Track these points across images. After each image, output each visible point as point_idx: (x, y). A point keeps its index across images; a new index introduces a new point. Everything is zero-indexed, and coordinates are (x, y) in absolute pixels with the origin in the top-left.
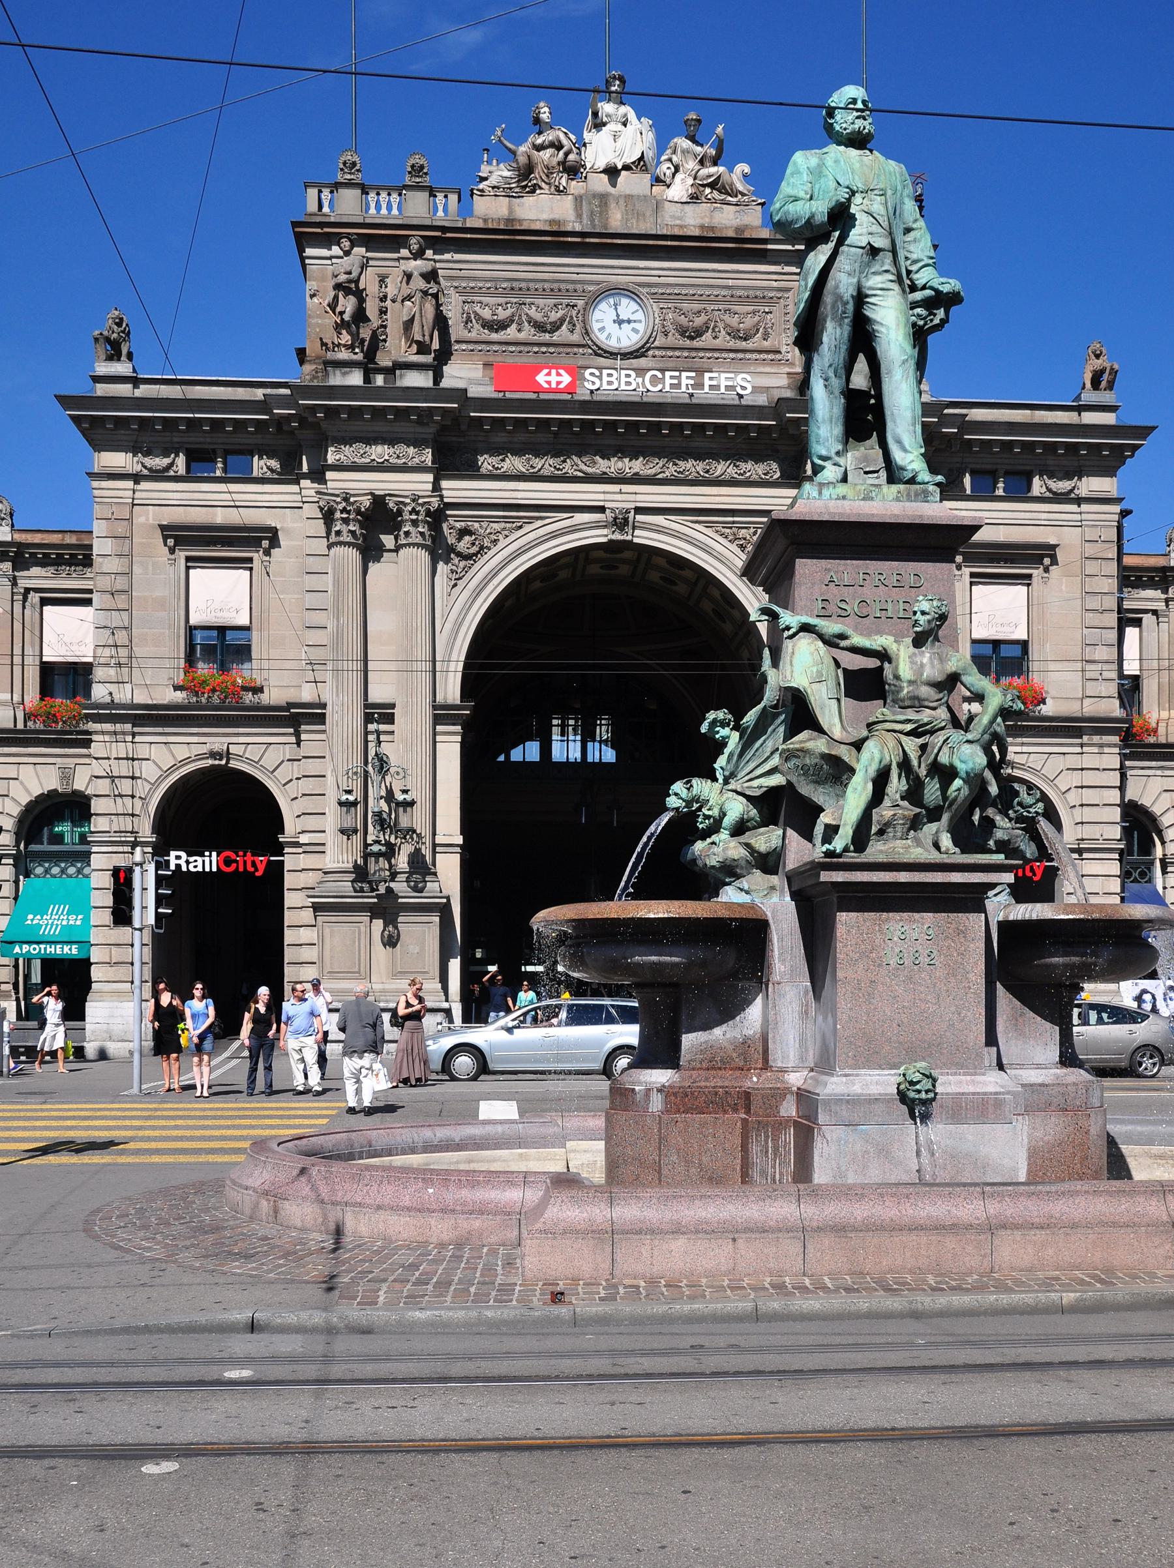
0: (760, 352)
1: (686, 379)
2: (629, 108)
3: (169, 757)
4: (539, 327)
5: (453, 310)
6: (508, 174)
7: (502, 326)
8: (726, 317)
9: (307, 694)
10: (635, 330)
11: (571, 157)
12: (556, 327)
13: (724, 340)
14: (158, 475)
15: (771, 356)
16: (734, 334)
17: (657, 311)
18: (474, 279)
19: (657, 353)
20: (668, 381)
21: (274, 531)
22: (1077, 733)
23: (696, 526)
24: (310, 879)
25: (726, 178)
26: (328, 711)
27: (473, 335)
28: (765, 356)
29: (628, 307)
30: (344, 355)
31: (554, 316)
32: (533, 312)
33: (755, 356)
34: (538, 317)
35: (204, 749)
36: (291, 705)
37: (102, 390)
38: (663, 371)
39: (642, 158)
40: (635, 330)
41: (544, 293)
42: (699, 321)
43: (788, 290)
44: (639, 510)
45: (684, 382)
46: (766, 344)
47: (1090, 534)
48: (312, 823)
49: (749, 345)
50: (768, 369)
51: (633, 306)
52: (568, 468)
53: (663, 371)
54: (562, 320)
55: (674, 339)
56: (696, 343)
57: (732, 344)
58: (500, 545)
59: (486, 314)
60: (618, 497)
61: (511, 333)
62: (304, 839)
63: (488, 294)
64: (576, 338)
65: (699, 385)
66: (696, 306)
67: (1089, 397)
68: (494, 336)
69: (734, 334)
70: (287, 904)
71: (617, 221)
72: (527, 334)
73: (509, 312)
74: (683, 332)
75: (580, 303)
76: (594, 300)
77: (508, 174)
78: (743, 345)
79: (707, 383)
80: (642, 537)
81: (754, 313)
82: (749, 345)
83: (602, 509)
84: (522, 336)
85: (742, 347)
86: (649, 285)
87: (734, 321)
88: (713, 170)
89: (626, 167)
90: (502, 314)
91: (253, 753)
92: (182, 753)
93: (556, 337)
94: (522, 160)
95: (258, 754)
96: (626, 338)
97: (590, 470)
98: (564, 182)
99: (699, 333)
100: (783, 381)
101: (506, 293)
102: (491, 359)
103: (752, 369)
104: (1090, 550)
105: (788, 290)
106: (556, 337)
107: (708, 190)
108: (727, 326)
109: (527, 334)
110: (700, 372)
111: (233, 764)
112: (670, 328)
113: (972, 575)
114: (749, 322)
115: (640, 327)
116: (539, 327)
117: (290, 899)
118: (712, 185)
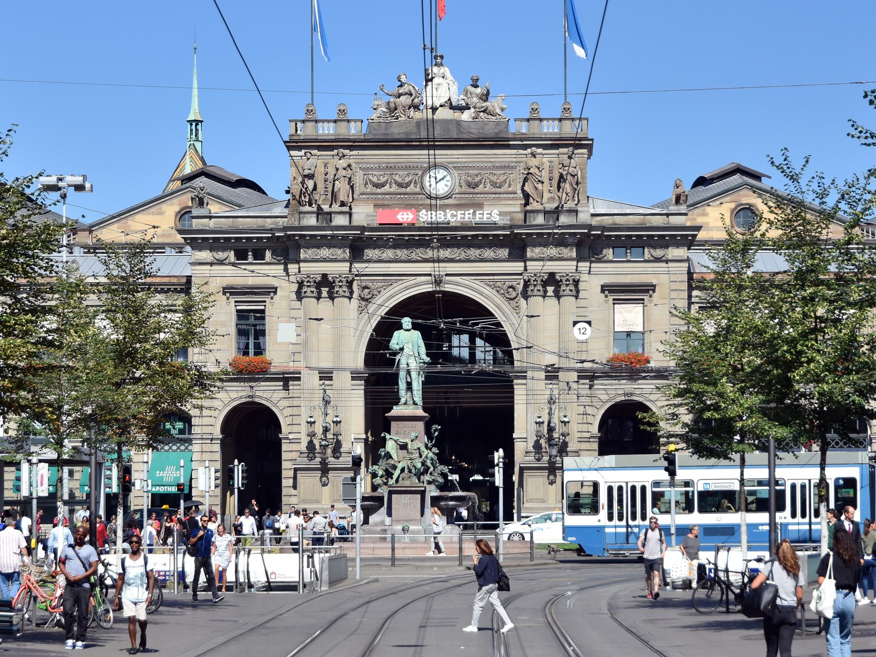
0: (507, 193)
2: (446, 68)
4: (400, 185)
5: (358, 180)
6: (385, 110)
7: (383, 185)
9: (292, 366)
10: (446, 185)
11: (416, 100)
12: (408, 185)
14: (221, 262)
15: (512, 196)
17: (456, 175)
18: (370, 163)
19: (457, 196)
21: (276, 288)
23: (476, 282)
24: (295, 455)
25: (490, 108)
26: (302, 376)
27: (369, 190)
28: (509, 196)
29: (441, 173)
31: (407, 180)
32: (397, 178)
33: (505, 196)
34: (400, 180)
36: (284, 373)
39: (449, 99)
40: (446, 185)
41: (402, 169)
42: (477, 179)
43: (520, 162)
44: (447, 275)
46: (510, 189)
47: (673, 278)
48: (295, 428)
49: (502, 190)
50: (511, 202)
52: (414, 256)
54: (411, 182)
55: (465, 189)
56: (476, 190)
57: (493, 190)
58: (382, 293)
59: (375, 179)
61: (387, 188)
62: (291, 436)
63: (376, 169)
64: (418, 190)
67: (673, 209)
68: (379, 191)
69: (494, 184)
70: (283, 467)
71: (438, 133)
72: (394, 189)
73: (386, 178)
74: (469, 185)
75: (420, 173)
77: (385, 110)
81: (504, 174)
82: (502, 190)
84: (392, 190)
86: (453, 163)
87: (494, 179)
88: (484, 104)
89: (441, 106)
90: (383, 180)
91: (266, 395)
92: (234, 395)
93: (408, 190)
94: (392, 105)
95: (268, 394)
96: (442, 188)
97: (424, 257)
98: (412, 113)
99: (477, 185)
101: (384, 169)
102: (378, 202)
103: (503, 202)
104: (674, 286)
105: (520, 162)
106: (408, 190)
107: (482, 114)
108: (491, 181)
109: (394, 189)
111: (257, 400)
112: (463, 184)
115: (449, 184)
116: (400, 185)
117: (285, 465)
118: (484, 111)
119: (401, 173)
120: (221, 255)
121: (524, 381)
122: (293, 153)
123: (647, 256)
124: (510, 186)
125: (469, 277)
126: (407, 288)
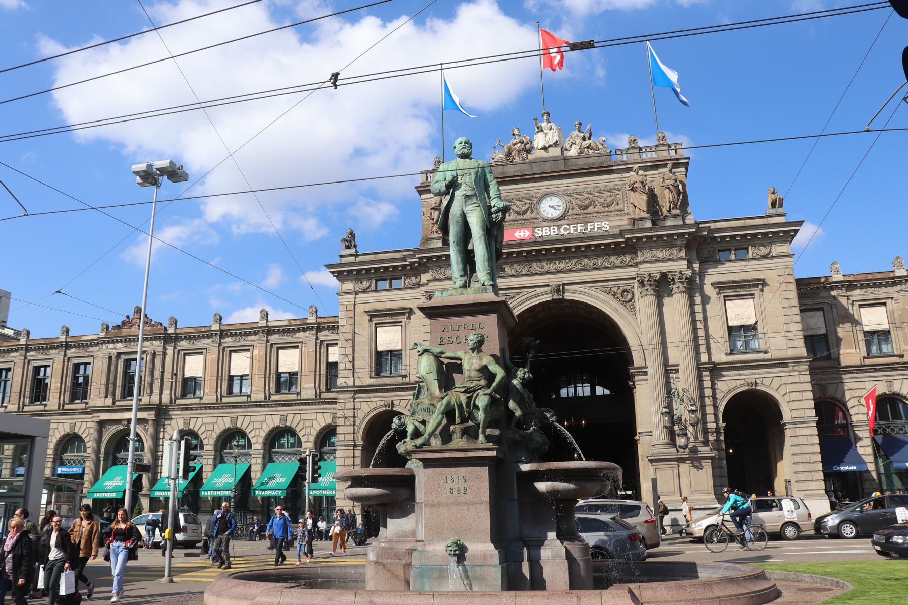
1: (580, 227)
3: (369, 407)
4: (518, 213)
8: (599, 199)
12: (525, 212)
13: (599, 208)
14: (365, 291)
16: (602, 204)
20: (572, 229)
22: (785, 365)
30: (435, 235)
31: (524, 208)
34: (517, 209)
35: (382, 403)
37: (344, 260)
38: (569, 225)
41: (519, 199)
42: (586, 202)
45: (579, 228)
51: (558, 200)
53: (569, 225)
54: (527, 210)
57: (602, 209)
60: (556, 280)
64: (533, 216)
65: (586, 229)
66: (585, 196)
69: (602, 204)
74: (580, 207)
76: (540, 200)
78: (607, 209)
79: (589, 228)
80: (568, 296)
83: (548, 286)
85: (608, 209)
87: (602, 200)
93: (525, 217)
96: (555, 214)
99: (587, 207)
100: (626, 222)
106: (525, 217)
110: (585, 223)
113: (725, 297)
114: (609, 200)
119: (518, 203)
120: (365, 284)
121: (645, 377)
122: (423, 196)
123: (750, 255)
124: (617, 204)
125: (587, 288)
126: (528, 299)
